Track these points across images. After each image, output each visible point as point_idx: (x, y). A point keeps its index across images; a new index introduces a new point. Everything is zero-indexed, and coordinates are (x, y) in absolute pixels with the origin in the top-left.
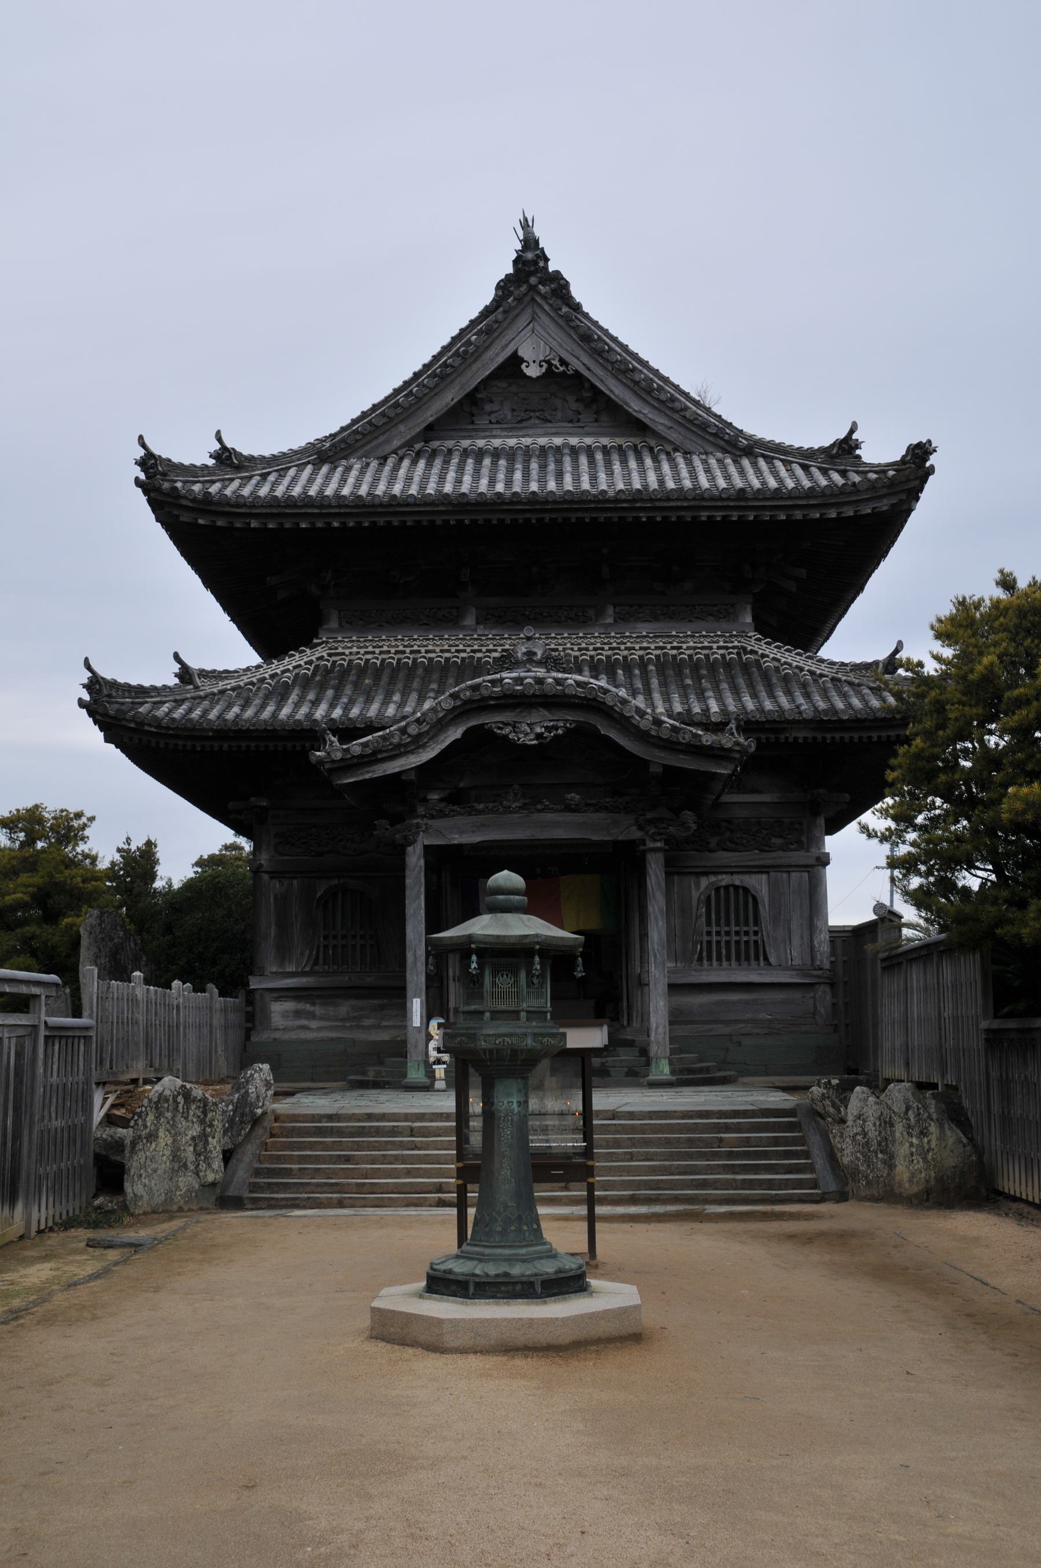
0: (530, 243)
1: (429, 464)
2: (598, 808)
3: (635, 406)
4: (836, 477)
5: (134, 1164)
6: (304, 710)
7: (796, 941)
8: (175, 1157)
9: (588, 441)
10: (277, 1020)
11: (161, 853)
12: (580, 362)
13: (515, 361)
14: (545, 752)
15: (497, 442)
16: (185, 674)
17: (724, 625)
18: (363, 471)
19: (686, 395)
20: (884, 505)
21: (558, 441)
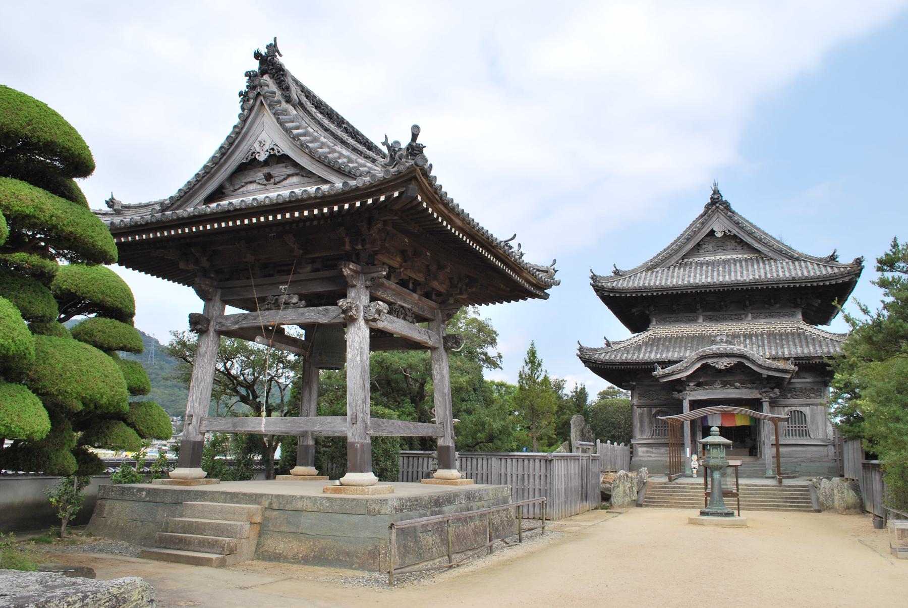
0: (716, 192)
1: (685, 269)
2: (746, 388)
3: (756, 245)
4: (829, 269)
5: (614, 493)
6: (647, 355)
7: (820, 430)
8: (624, 492)
9: (740, 256)
10: (640, 454)
11: (587, 390)
12: (735, 231)
13: (712, 233)
14: (729, 371)
15: (707, 259)
16: (608, 344)
17: (791, 319)
18: (662, 274)
19: (774, 239)
20: (847, 279)
21: (729, 257)
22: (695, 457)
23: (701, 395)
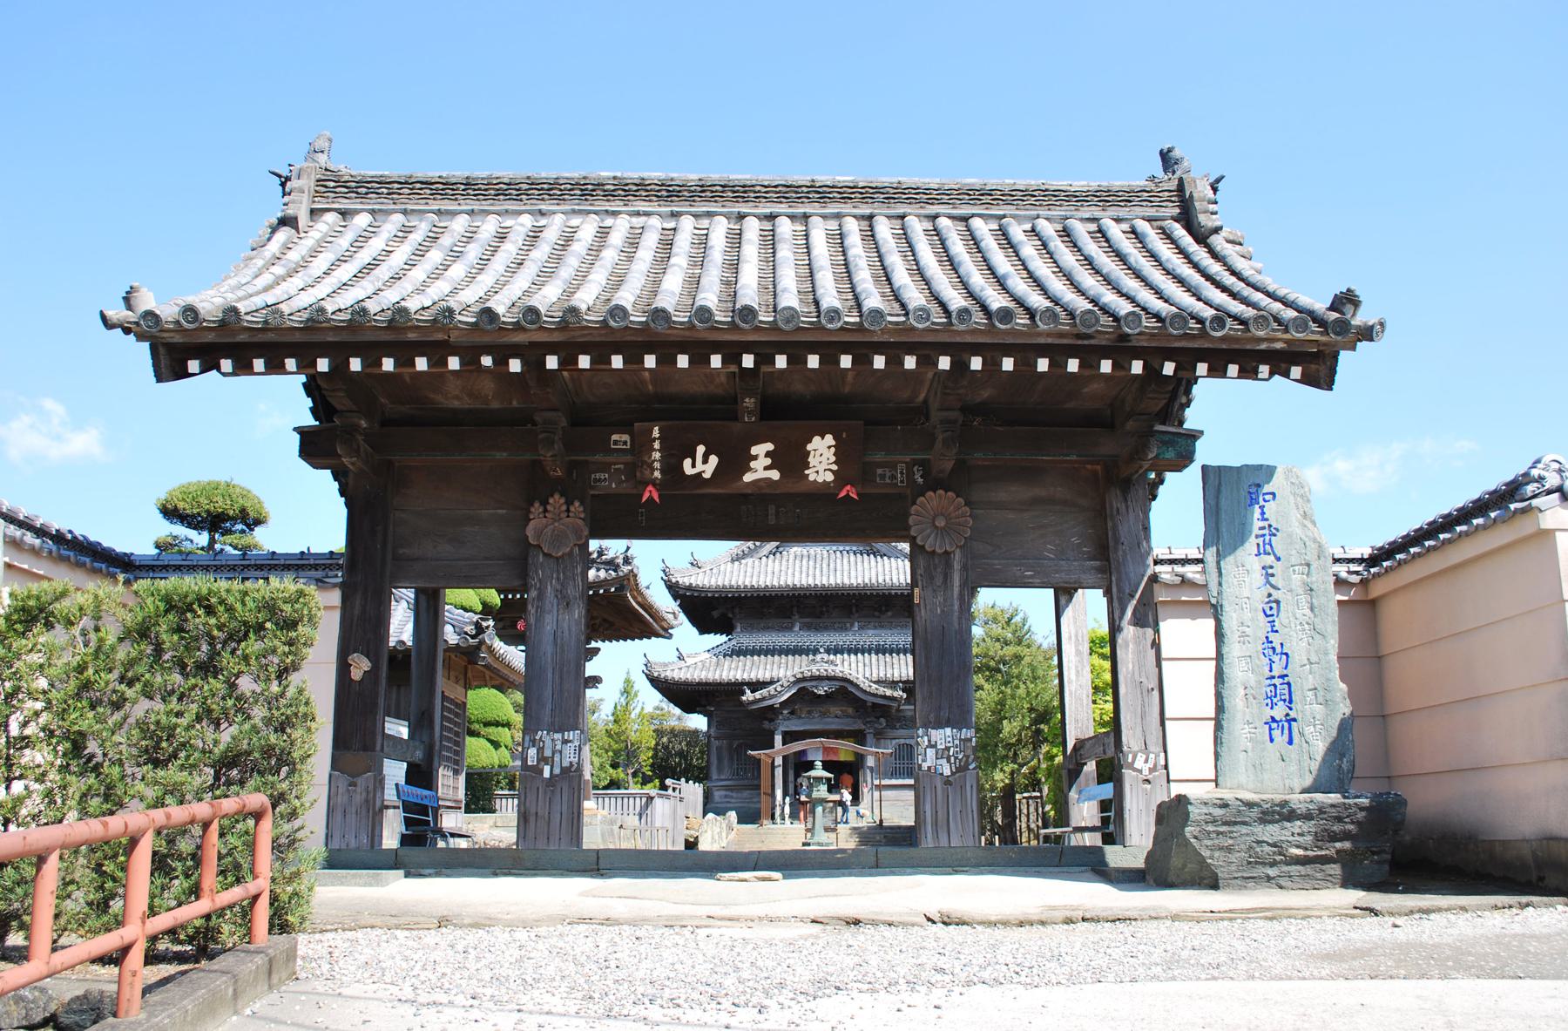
14: (828, 696)
16: (681, 658)
23: (795, 726)
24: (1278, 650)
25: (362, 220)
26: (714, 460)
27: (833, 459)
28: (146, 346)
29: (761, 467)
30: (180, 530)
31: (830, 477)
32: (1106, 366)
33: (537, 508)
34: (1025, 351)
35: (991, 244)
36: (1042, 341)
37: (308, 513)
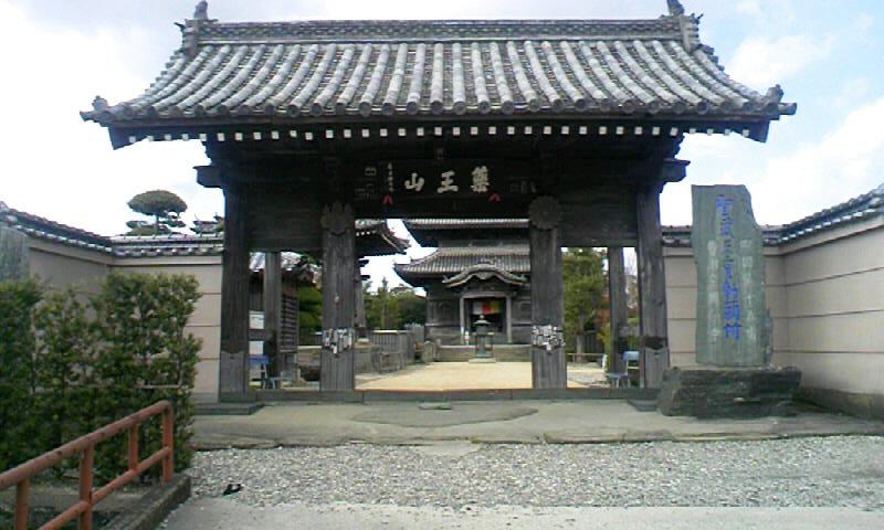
14: (487, 280)
22: (467, 333)
23: (471, 295)
24: (732, 287)
25: (224, 50)
26: (422, 181)
27: (486, 179)
28: (106, 129)
29: (447, 185)
30: (139, 217)
31: (485, 190)
32: (639, 131)
33: (326, 208)
34: (593, 125)
35: (571, 57)
36: (602, 117)
37: (208, 205)
